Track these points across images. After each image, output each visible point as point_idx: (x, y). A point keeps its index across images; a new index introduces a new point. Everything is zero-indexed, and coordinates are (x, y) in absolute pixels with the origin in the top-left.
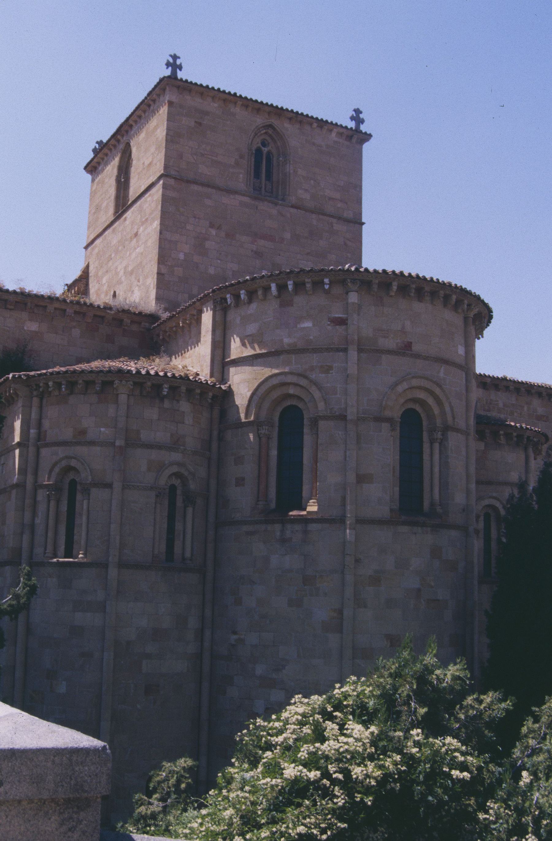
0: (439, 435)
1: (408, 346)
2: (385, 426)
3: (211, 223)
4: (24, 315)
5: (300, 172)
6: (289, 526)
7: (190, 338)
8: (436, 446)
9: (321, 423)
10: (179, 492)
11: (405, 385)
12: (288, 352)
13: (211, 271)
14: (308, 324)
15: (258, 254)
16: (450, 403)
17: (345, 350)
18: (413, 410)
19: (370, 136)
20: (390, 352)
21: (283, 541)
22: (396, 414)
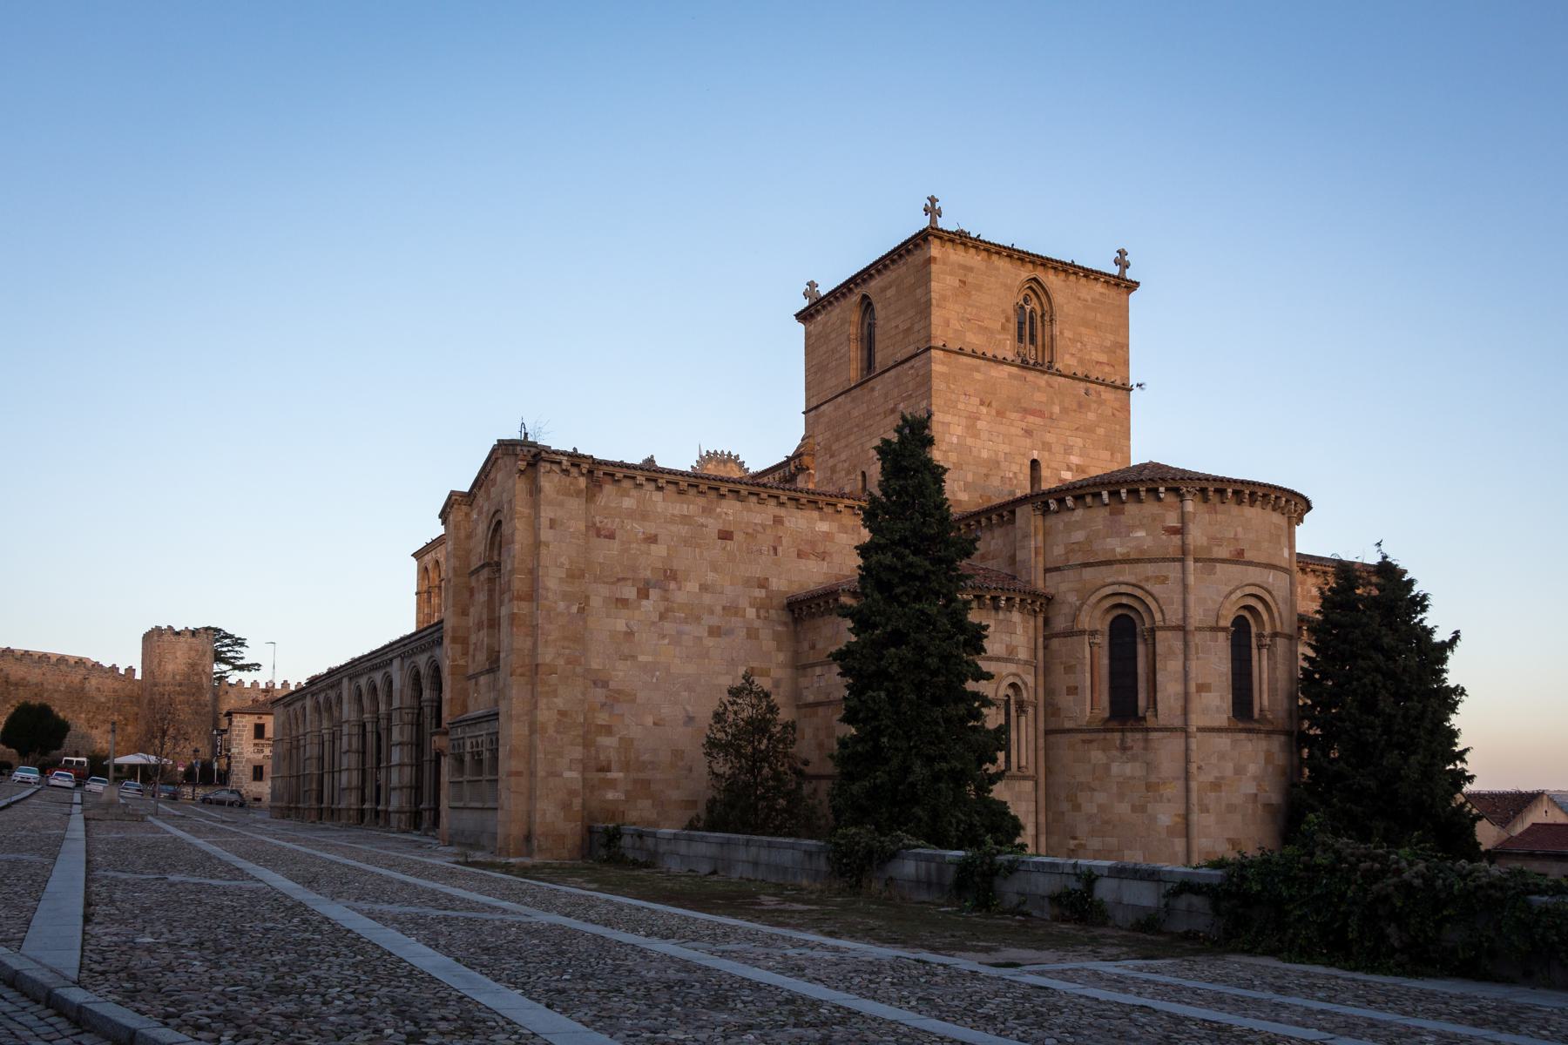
0: (1268, 641)
1: (1241, 553)
2: (1221, 635)
3: (981, 400)
4: (815, 514)
5: (1067, 334)
6: (1129, 734)
7: (993, 538)
8: (1265, 651)
9: (1159, 634)
10: (1012, 702)
11: (1239, 594)
12: (1120, 562)
13: (985, 454)
14: (1141, 534)
15: (1028, 433)
16: (1278, 608)
17: (1182, 560)
18: (1242, 617)
19: (1138, 284)
20: (1223, 561)
21: (1124, 748)
22: (1226, 622)
